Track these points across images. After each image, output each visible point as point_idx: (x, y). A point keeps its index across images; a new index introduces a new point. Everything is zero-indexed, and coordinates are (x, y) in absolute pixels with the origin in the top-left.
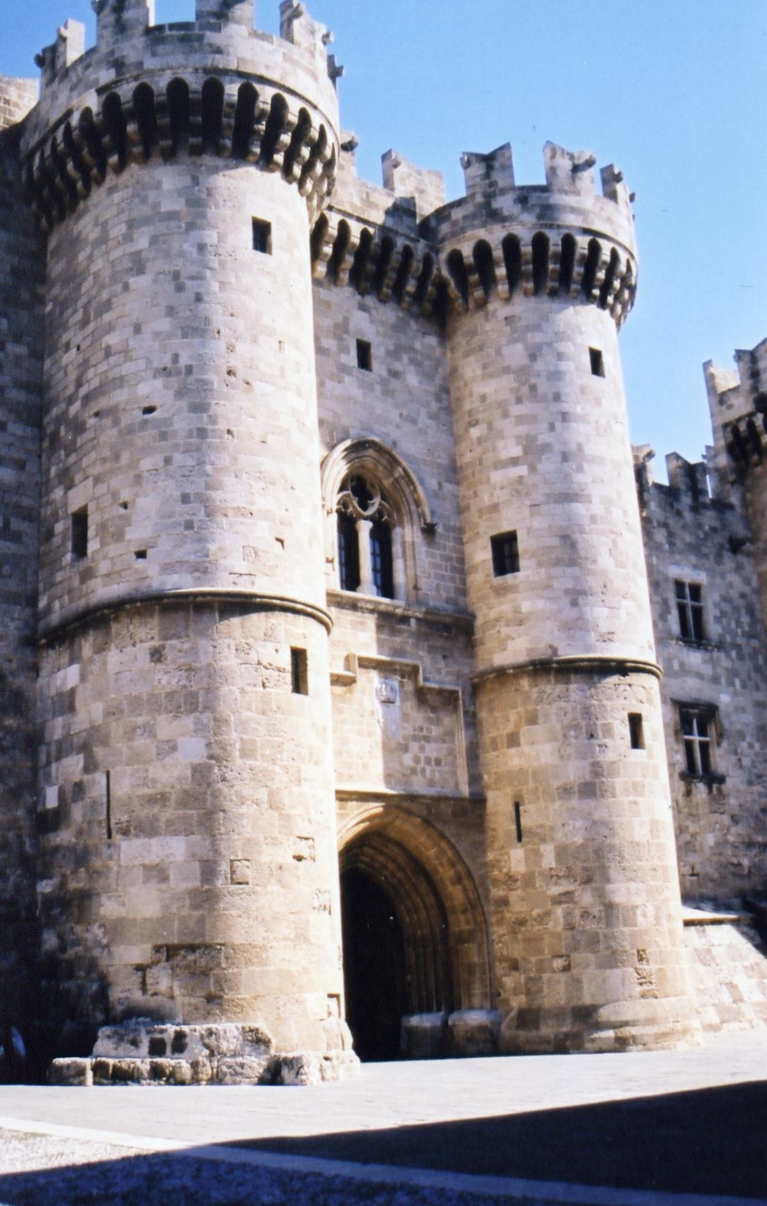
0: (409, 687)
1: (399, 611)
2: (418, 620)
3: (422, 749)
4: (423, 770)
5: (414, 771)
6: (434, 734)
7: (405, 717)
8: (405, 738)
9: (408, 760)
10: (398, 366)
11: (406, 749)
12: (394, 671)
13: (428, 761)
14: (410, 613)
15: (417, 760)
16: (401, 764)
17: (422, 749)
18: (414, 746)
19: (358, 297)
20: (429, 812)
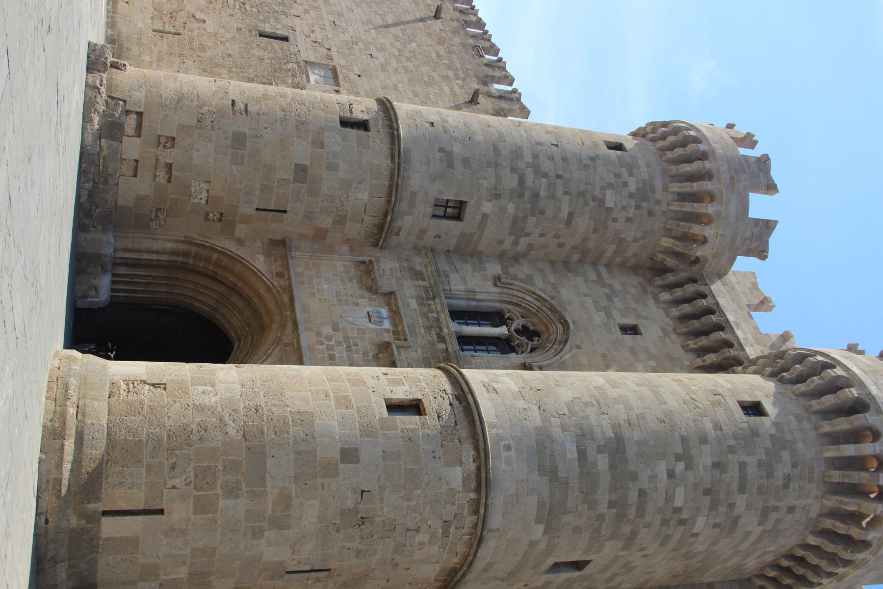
0: (388, 338)
1: (445, 330)
2: (447, 350)
3: (339, 344)
4: (322, 343)
5: (319, 334)
6: (355, 356)
7: (362, 332)
8: (344, 329)
9: (327, 330)
10: (642, 357)
11: (336, 329)
12: (395, 325)
13: (330, 348)
14: (448, 340)
15: (329, 338)
16: (322, 324)
17: (339, 344)
18: (340, 337)
19: (670, 329)
20: (286, 345)
